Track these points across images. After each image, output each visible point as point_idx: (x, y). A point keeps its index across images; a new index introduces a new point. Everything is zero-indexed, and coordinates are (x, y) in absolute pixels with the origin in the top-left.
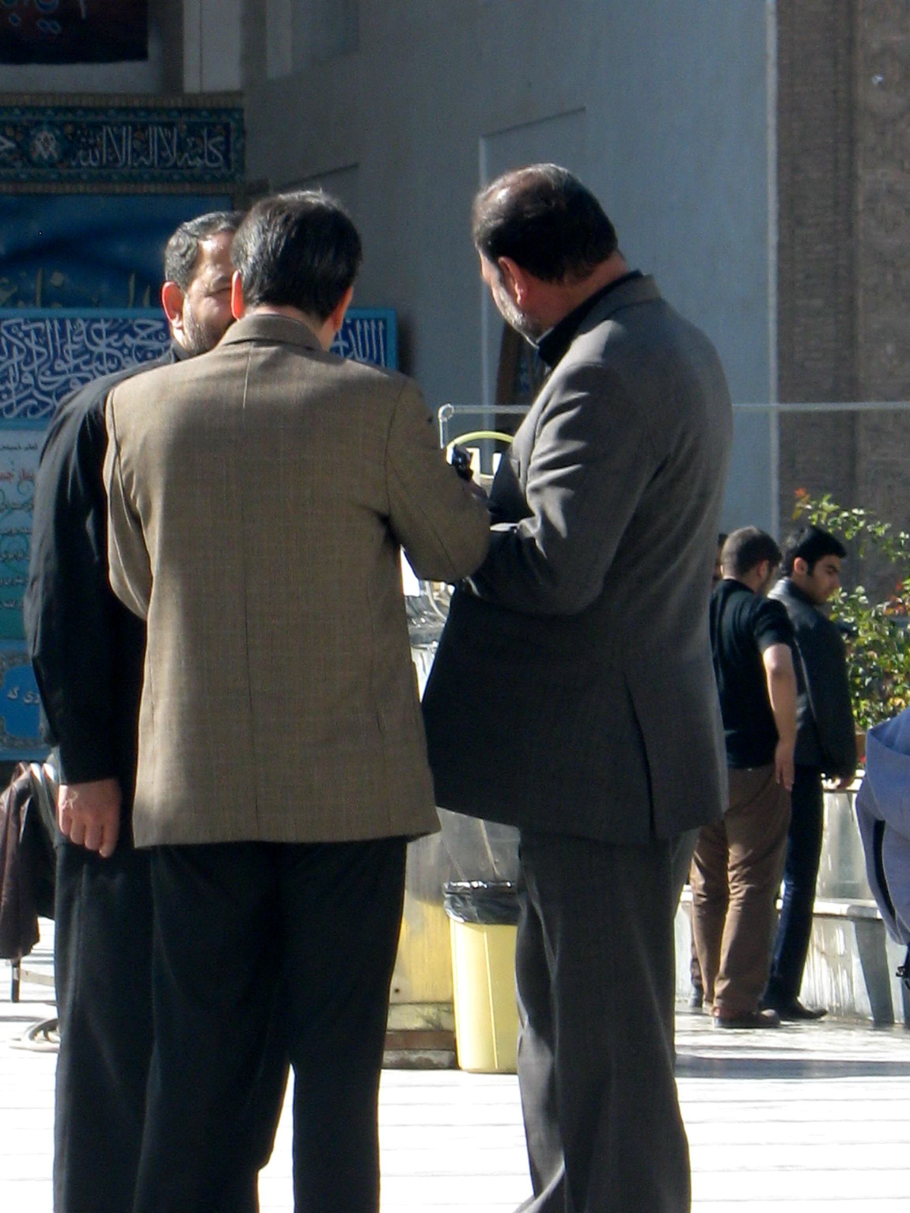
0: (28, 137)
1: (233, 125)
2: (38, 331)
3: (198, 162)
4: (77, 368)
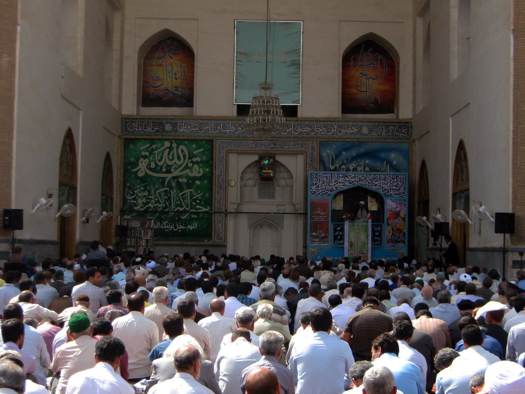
0: (361, 129)
1: (410, 126)
2: (326, 176)
3: (401, 135)
4: (335, 185)
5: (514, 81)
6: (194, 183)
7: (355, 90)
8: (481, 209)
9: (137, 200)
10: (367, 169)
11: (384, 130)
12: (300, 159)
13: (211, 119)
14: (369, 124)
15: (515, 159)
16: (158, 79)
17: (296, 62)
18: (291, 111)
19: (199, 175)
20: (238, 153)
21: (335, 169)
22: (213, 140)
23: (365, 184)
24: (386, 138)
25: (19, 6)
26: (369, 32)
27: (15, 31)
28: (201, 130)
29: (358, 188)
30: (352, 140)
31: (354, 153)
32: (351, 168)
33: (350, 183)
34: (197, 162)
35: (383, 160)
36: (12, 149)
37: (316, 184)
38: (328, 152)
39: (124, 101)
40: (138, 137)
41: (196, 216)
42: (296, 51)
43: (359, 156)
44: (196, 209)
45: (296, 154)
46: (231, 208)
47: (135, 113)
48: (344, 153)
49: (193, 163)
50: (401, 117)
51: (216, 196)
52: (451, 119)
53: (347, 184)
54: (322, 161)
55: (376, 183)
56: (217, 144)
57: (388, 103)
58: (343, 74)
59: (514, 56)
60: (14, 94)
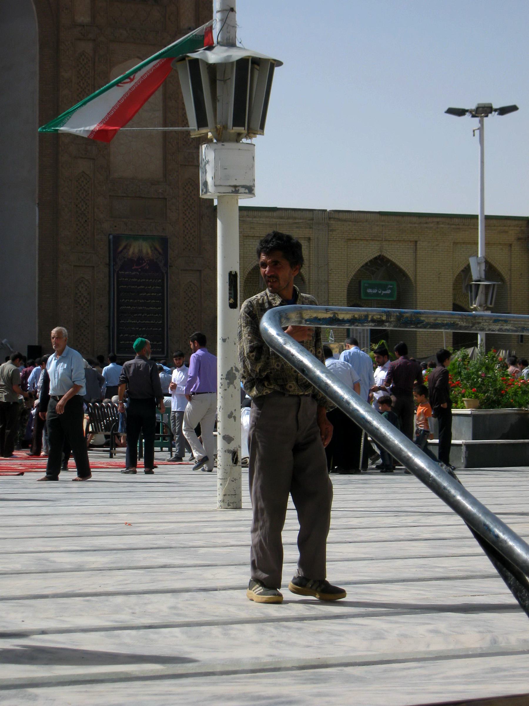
5: (39, 244)
8: (3, 342)
59: (39, 224)
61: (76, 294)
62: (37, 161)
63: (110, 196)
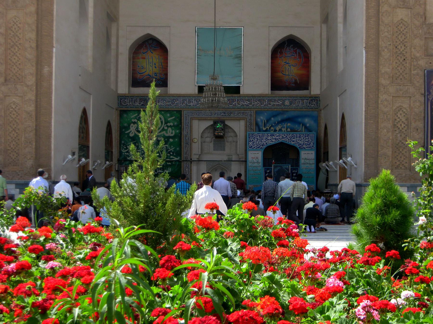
5: (366, 80)
6: (168, 140)
7: (280, 74)
9: (129, 153)
10: (289, 130)
11: (301, 103)
12: (242, 123)
13: (180, 96)
14: (290, 98)
15: (366, 128)
16: (143, 68)
17: (239, 56)
18: (236, 90)
19: (172, 135)
20: (199, 120)
21: (266, 131)
22: (181, 111)
23: (286, 140)
24: (301, 108)
25: (54, 35)
26: (290, 34)
27: (53, 52)
28: (173, 104)
29: (282, 143)
30: (278, 110)
31: (279, 118)
32: (278, 129)
33: (276, 140)
34: (170, 126)
35: (299, 123)
36: (51, 125)
37: (253, 141)
38: (262, 118)
39: (119, 84)
40: (129, 109)
41: (170, 164)
42: (239, 48)
43: (283, 121)
44: (170, 158)
45: (239, 119)
46: (195, 158)
47: (127, 93)
48: (272, 119)
49: (167, 126)
50: (312, 93)
51: (184, 150)
52: (338, 98)
53: (274, 140)
54: (257, 124)
55: (294, 140)
56: (184, 113)
57: (304, 83)
58: (272, 63)
60: (52, 91)
61: (396, 120)
62: (364, 12)
63: (426, 38)
